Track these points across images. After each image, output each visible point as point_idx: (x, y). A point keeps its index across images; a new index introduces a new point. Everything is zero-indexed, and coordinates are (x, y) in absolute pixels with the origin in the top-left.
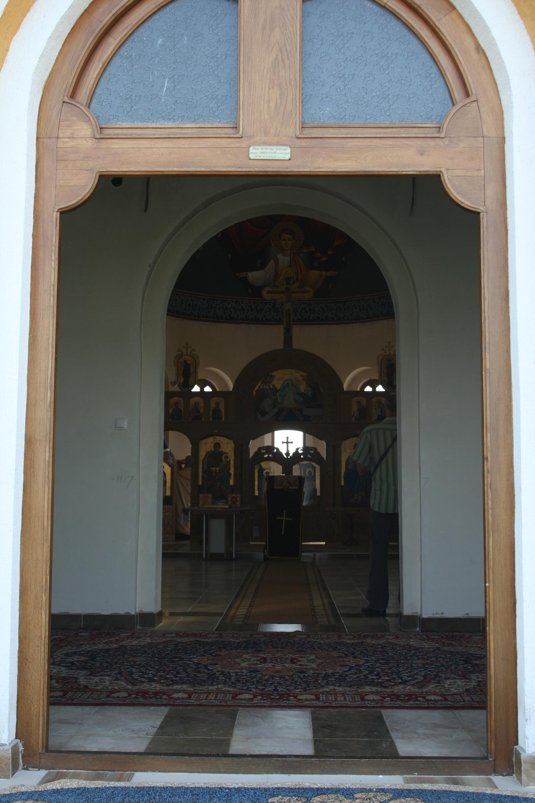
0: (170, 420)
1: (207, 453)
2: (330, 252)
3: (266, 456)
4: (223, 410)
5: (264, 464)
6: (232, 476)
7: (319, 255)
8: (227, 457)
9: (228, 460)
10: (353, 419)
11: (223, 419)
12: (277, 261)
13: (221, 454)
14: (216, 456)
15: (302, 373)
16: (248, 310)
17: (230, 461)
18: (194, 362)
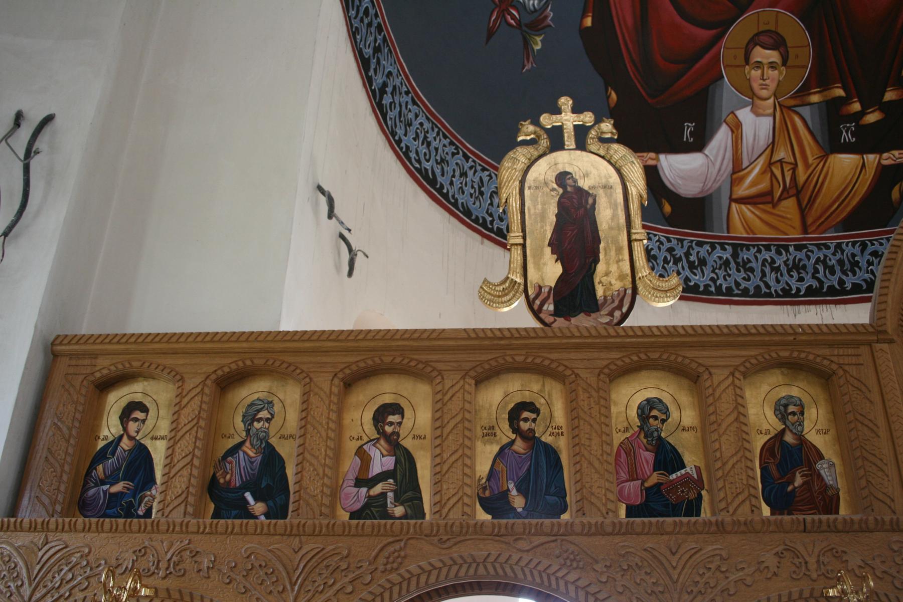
0: (483, 516)
7: (856, 107)
11: (843, 511)
12: (736, 128)
16: (666, 261)
18: (615, 178)
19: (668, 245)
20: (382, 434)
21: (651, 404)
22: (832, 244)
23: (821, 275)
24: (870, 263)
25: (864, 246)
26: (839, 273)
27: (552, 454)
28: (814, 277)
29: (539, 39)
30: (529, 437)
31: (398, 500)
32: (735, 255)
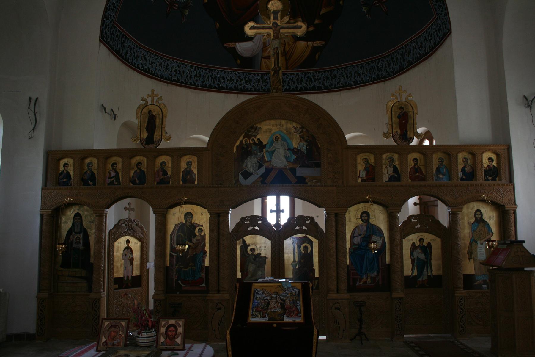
1: (176, 225)
2: (316, 22)
3: (250, 228)
4: (195, 171)
5: (248, 239)
6: (208, 254)
8: (201, 230)
9: (202, 234)
10: (359, 180)
11: (196, 183)
13: (194, 226)
14: (188, 229)
15: (295, 124)
16: (237, 81)
17: (205, 235)
18: (161, 113)
19: (238, 75)
20: (113, 168)
21: (163, 162)
22: (295, 73)
23: (290, 85)
24: (306, 81)
25: (305, 74)
26: (296, 84)
27: (144, 172)
28: (288, 85)
29: (187, 11)
30: (140, 169)
31: (116, 181)
32: (262, 77)
